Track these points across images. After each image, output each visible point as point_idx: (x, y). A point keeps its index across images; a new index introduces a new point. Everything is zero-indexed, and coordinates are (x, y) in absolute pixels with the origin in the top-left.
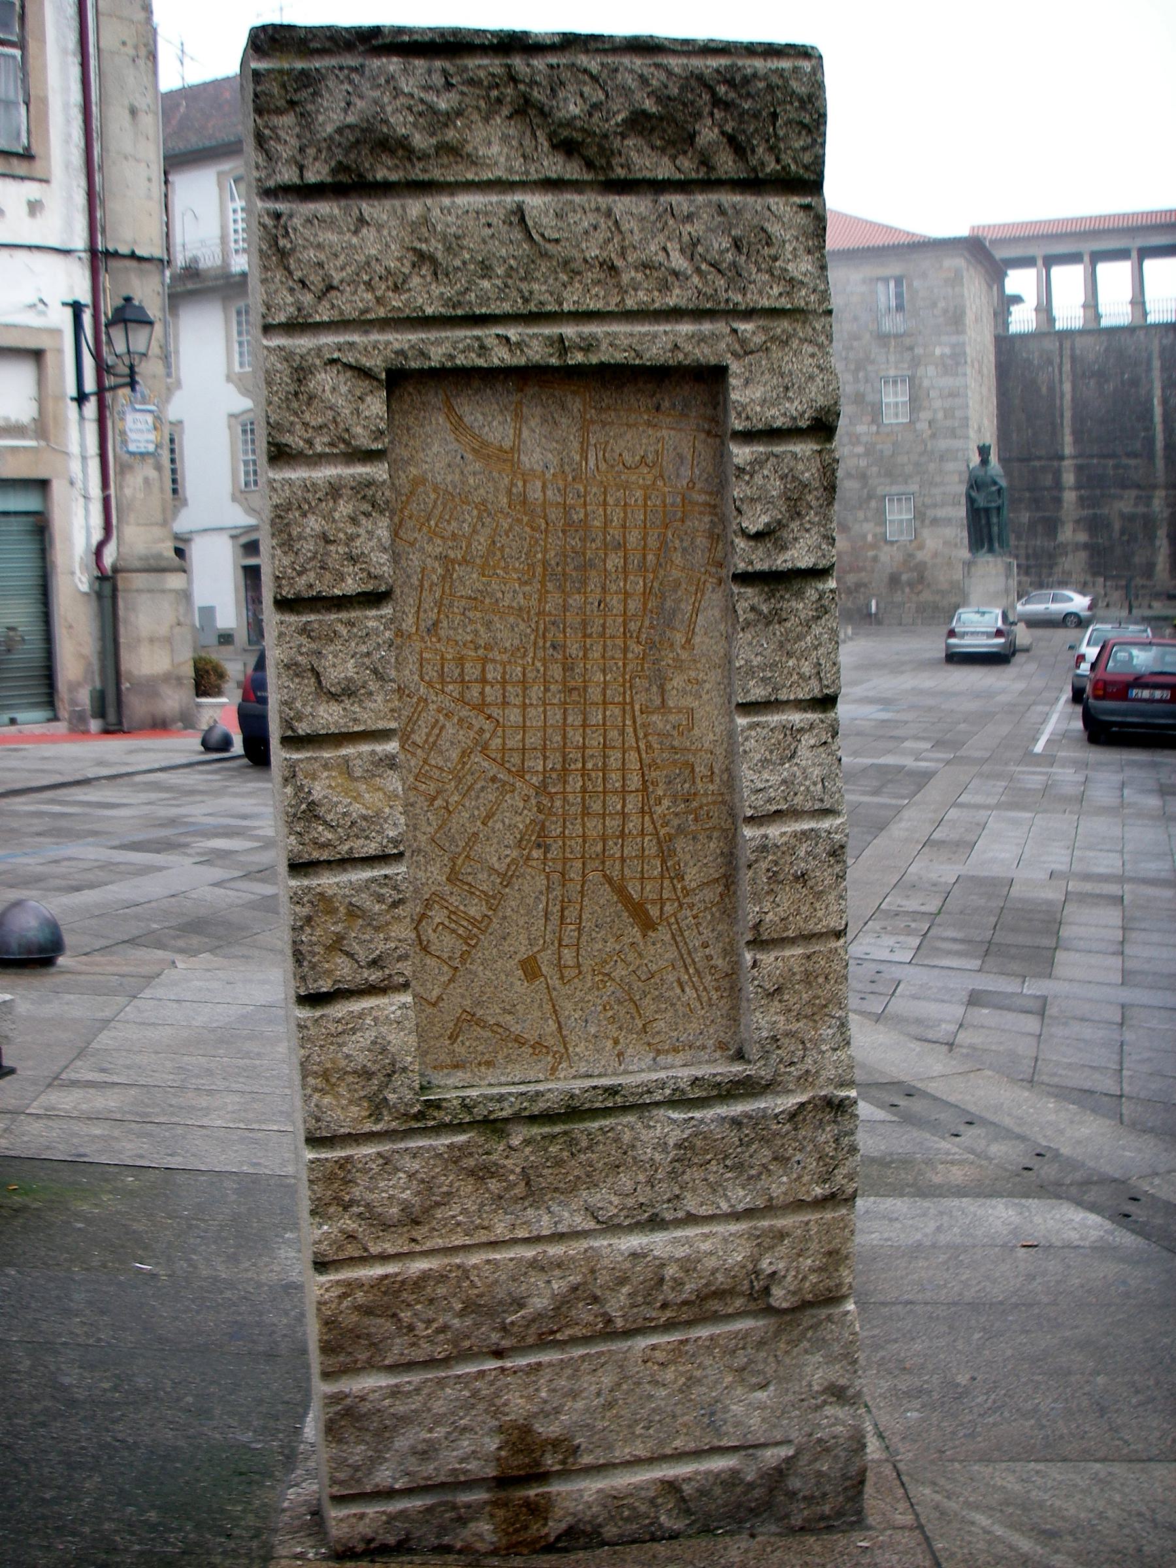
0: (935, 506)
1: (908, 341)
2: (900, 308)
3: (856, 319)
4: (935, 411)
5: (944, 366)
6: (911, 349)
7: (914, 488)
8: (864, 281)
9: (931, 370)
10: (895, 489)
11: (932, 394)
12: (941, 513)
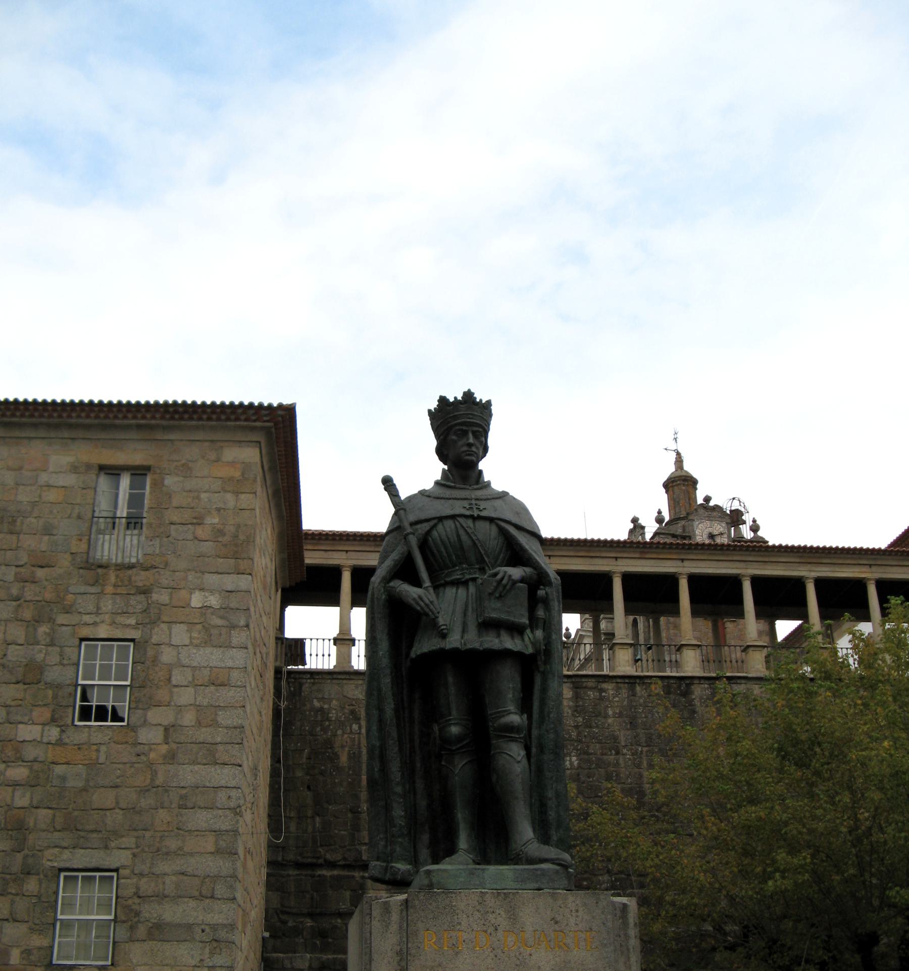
0: (161, 897)
1: (141, 578)
2: (134, 522)
3: (48, 531)
4: (180, 709)
5: (207, 629)
6: (145, 591)
7: (119, 858)
8: (74, 469)
9: (180, 634)
10: (81, 858)
11: (178, 677)
12: (170, 913)
